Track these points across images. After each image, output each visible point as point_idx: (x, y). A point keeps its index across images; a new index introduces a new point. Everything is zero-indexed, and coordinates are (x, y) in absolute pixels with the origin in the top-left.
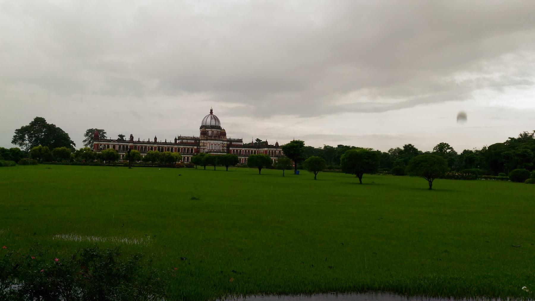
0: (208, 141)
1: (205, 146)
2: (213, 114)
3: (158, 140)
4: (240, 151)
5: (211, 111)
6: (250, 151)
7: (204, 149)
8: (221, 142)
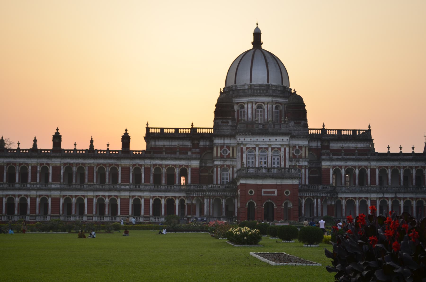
0: (241, 139)
1: (228, 157)
2: (263, 47)
3: (66, 145)
4: (363, 172)
5: (257, 35)
6: (402, 172)
7: (224, 169)
8: (285, 139)
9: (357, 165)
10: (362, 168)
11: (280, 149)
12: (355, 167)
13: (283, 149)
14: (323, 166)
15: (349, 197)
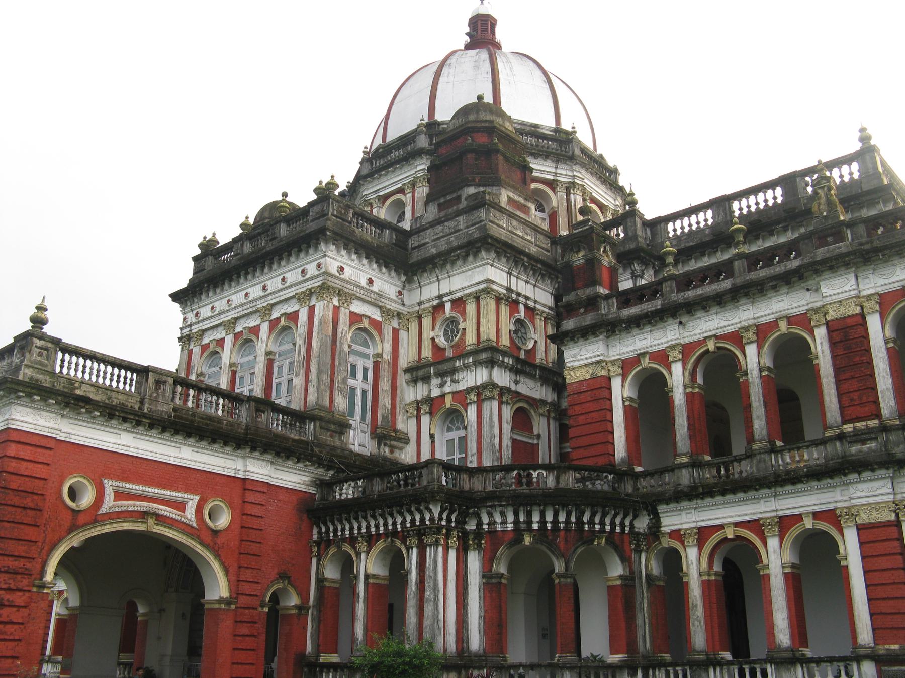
9: (744, 324)
10: (778, 334)
11: (293, 317)
12: (736, 338)
13: (303, 317)
14: (572, 373)
15: (721, 527)
